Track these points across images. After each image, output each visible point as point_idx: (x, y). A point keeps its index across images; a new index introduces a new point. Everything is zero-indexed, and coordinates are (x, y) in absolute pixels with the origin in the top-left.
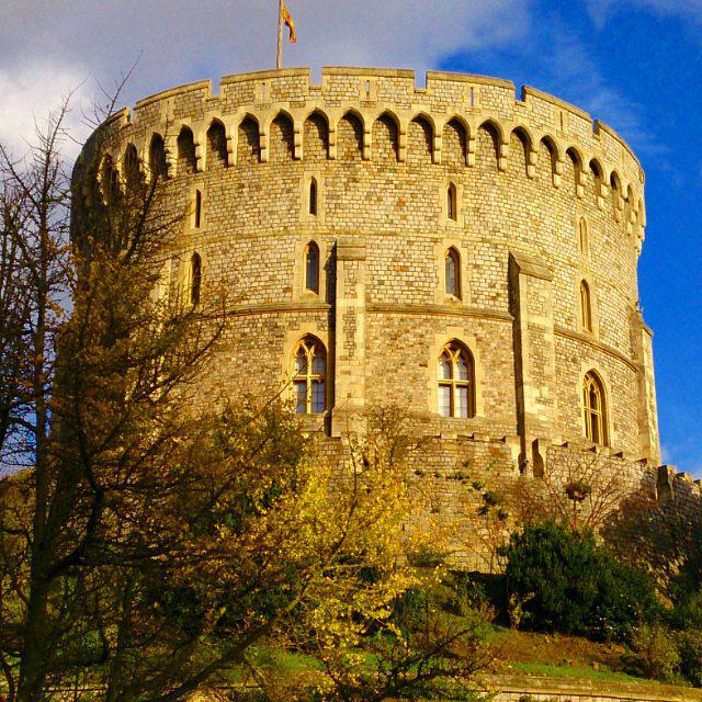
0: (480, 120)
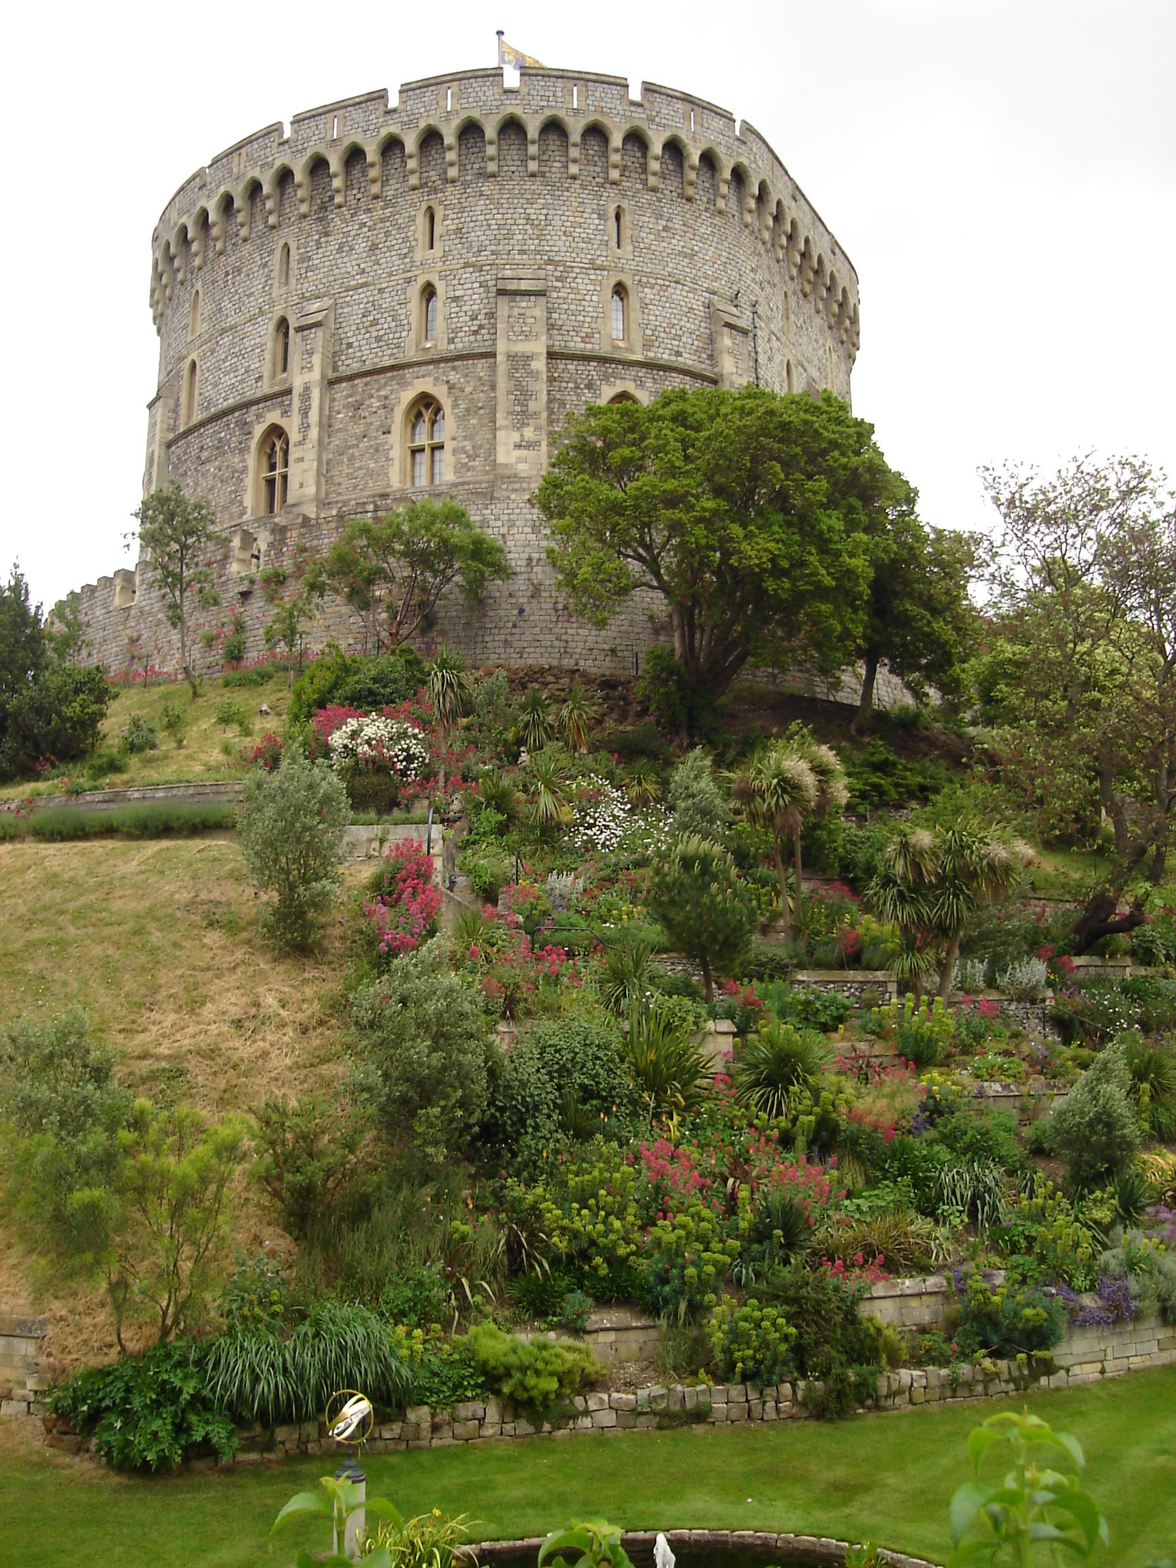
0: (456, 122)
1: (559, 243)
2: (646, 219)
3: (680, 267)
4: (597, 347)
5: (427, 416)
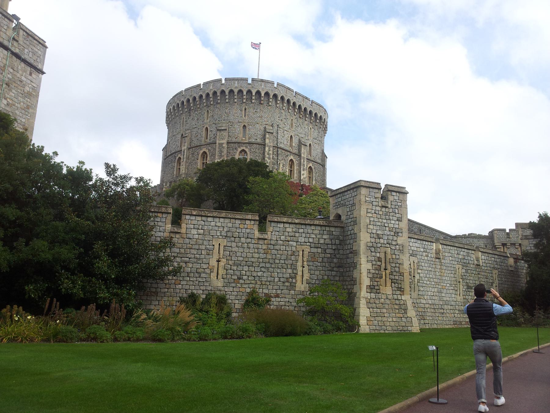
0: (212, 92)
1: (232, 118)
2: (251, 110)
3: (258, 120)
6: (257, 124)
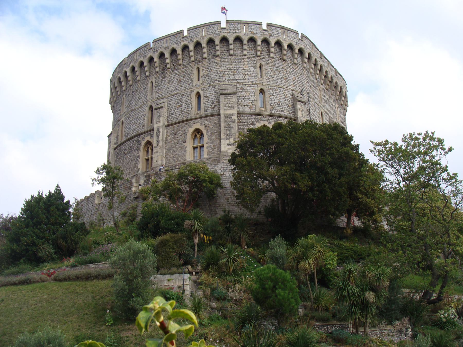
0: (206, 40)
2: (270, 67)
3: (282, 83)
4: (254, 110)
5: (198, 136)
6: (280, 89)
